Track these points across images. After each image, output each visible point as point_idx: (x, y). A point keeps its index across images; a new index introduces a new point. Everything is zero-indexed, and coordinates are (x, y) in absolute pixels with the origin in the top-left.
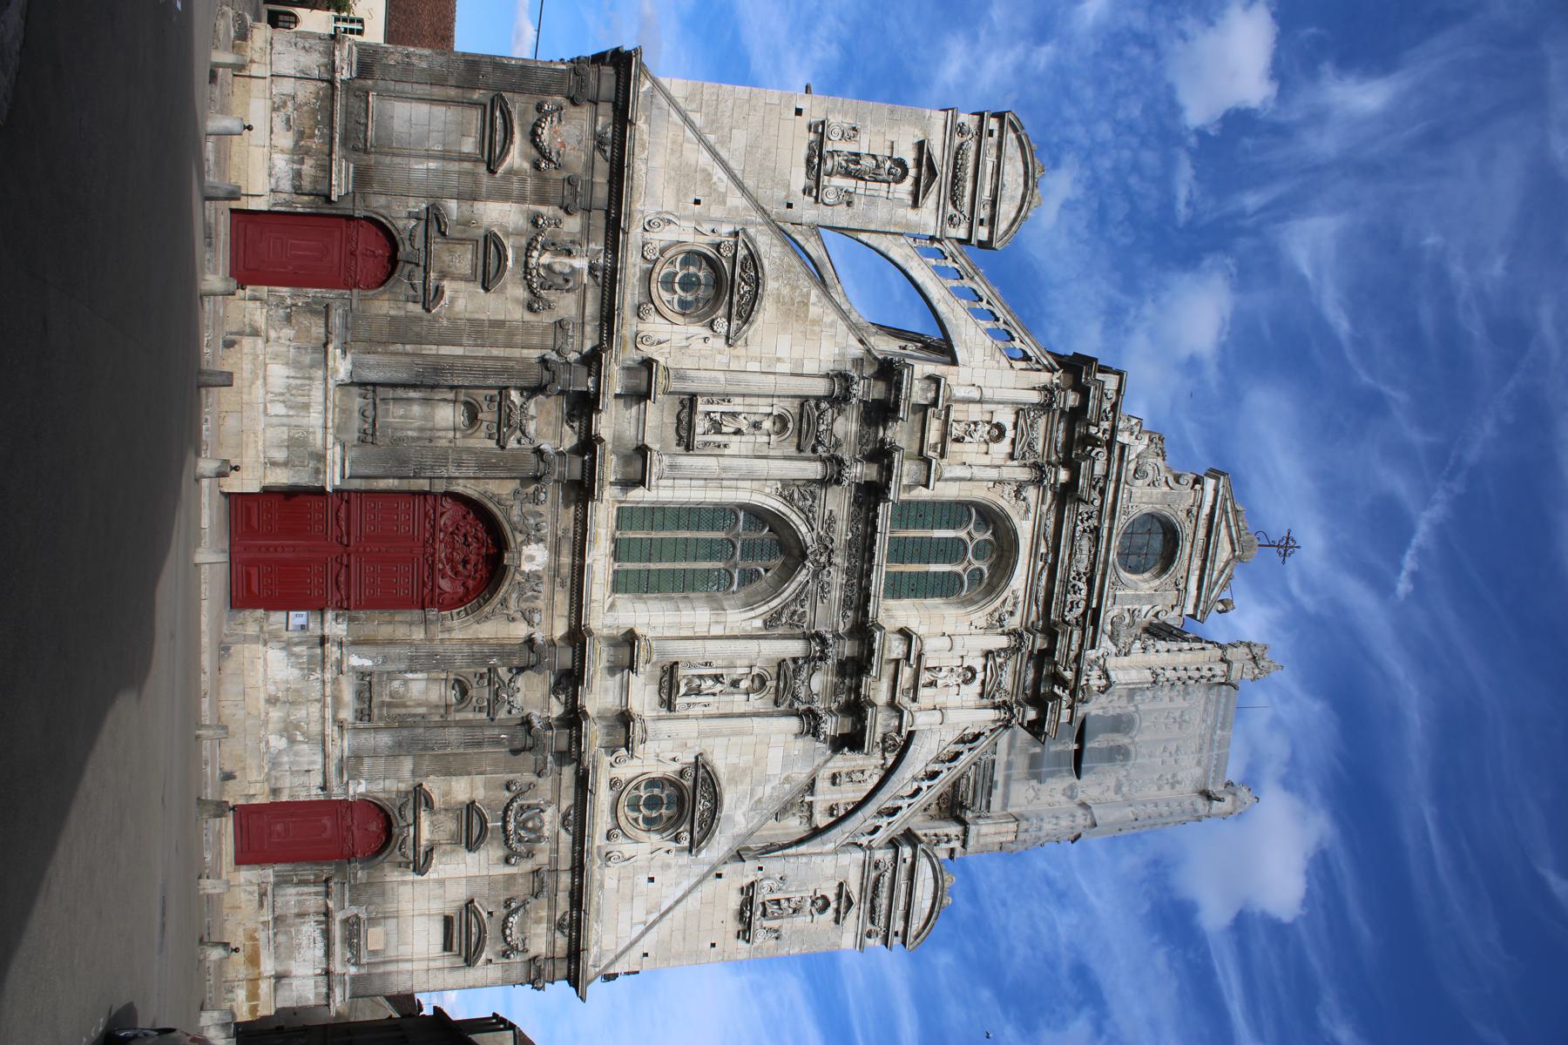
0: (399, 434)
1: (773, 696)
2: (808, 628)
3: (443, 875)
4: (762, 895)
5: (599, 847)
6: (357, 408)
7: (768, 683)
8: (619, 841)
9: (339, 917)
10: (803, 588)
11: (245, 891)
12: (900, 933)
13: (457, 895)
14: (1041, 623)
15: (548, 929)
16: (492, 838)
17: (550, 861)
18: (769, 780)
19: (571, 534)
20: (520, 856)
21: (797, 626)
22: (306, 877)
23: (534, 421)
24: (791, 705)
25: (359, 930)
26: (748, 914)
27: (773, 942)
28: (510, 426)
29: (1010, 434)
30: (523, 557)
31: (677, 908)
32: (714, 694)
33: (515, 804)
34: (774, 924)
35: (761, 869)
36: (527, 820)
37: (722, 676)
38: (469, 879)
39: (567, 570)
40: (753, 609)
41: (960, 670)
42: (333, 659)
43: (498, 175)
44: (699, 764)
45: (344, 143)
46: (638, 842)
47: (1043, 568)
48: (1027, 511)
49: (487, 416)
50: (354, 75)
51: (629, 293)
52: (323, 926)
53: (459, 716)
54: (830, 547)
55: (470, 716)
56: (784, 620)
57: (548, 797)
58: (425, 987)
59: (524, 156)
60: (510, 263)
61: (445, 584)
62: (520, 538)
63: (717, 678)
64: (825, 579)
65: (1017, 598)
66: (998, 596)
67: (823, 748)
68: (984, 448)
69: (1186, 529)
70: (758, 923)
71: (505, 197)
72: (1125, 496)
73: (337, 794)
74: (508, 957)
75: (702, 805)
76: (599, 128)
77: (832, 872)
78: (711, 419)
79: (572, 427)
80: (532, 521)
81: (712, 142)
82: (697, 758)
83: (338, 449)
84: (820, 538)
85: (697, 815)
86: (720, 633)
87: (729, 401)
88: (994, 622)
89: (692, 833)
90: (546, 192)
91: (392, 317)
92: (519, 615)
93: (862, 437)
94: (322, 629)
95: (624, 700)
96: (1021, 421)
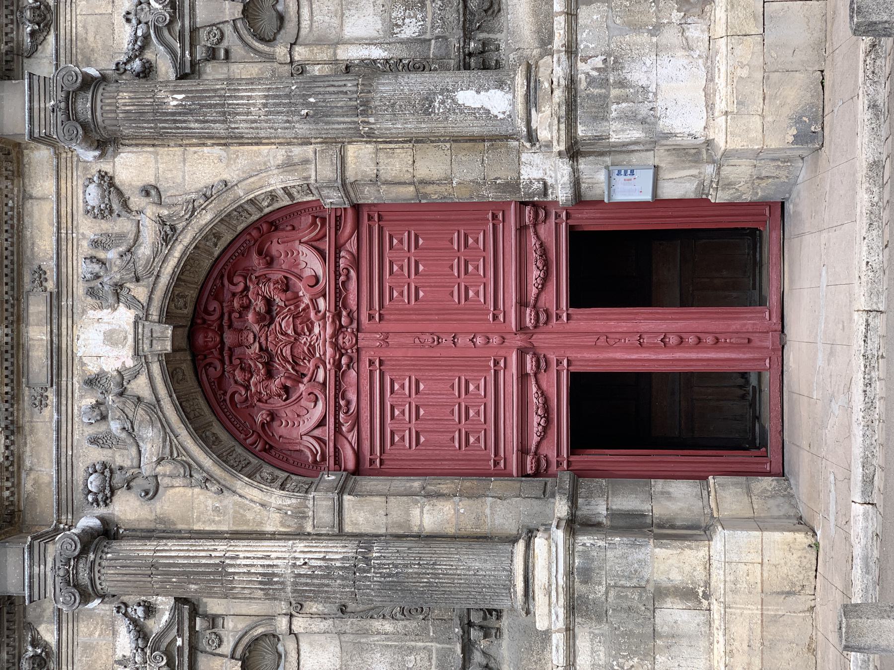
0: (412, 625)
23: (119, 655)
28: (167, 653)
30: (131, 338)
39: (32, 309)
42: (547, 110)
62: (140, 386)
79: (35, 643)
80: (115, 426)
92: (136, 201)
94: (575, 171)
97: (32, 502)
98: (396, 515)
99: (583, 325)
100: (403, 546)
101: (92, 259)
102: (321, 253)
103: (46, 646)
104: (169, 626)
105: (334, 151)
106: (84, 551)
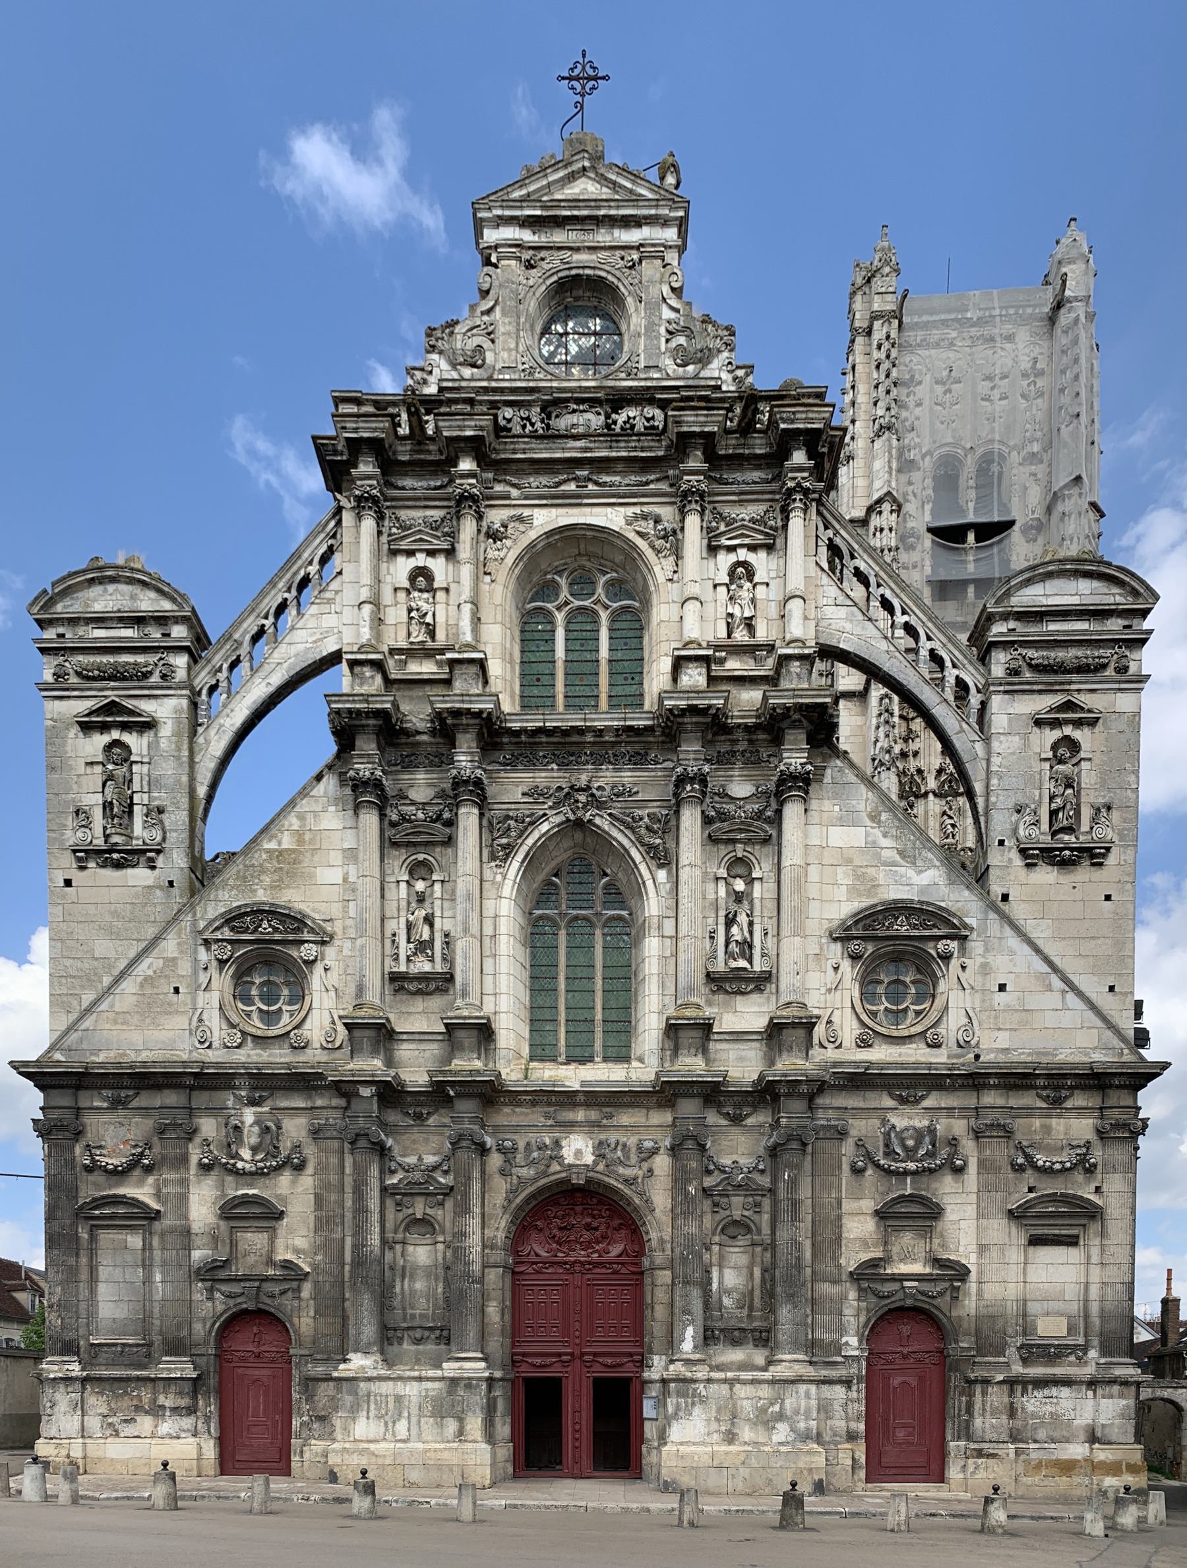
0: (441, 1302)
1: (757, 847)
2: (669, 808)
3: (974, 1248)
4: (1041, 835)
5: (949, 1057)
6: (413, 1347)
7: (740, 855)
8: (944, 1032)
9: (1018, 1369)
10: (618, 819)
11: (973, 1473)
12: (1126, 623)
13: (999, 1230)
14: (671, 472)
15: (1059, 1116)
16: (927, 1190)
17: (964, 1117)
18: (874, 842)
21: (667, 823)
22: (963, 1406)
23: (424, 1157)
24: (769, 821)
25: (1039, 1346)
26: (1067, 852)
27: (1115, 815)
29: (421, 560)
30: (578, 1162)
31: (1047, 950)
32: (751, 924)
33: (882, 1162)
34: (1086, 814)
35: (1001, 843)
37: (726, 916)
38: (980, 1216)
40: (644, 883)
41: (733, 587)
43: (162, 1210)
44: (843, 935)
45: (144, 1367)
46: (947, 1008)
47: (596, 483)
48: (520, 519)
49: (419, 1208)
50: (76, 1358)
51: (278, 1057)
52: (1030, 1387)
53: (766, 1230)
54: (566, 790)
56: (658, 841)
57: (877, 1122)
58: (1125, 1268)
59: (141, 1183)
60: (251, 1192)
62: (555, 1167)
63: (730, 921)
64: (608, 788)
65: (636, 517)
66: (635, 547)
67: (834, 770)
68: (440, 595)
69: (552, 261)
70: (1082, 838)
71: (183, 1200)
72: (507, 377)
73: (858, 1370)
74: (1095, 1166)
76: (105, 1105)
77: (1017, 738)
78: (415, 954)
79: (428, 1113)
80: (535, 1154)
81: (111, 979)
82: (835, 940)
84: (555, 806)
87: (394, 935)
88: (668, 545)
90: (176, 1158)
91: (316, 1312)
93: (432, 764)
95: (755, 1037)
96: (404, 545)
97: (498, 1112)
98: (493, 1294)
99: (584, 1384)
100: (479, 1299)
101: (618, 1143)
102: (620, 1256)
103: (427, 1119)
104: (440, 1183)
106: (475, 1144)
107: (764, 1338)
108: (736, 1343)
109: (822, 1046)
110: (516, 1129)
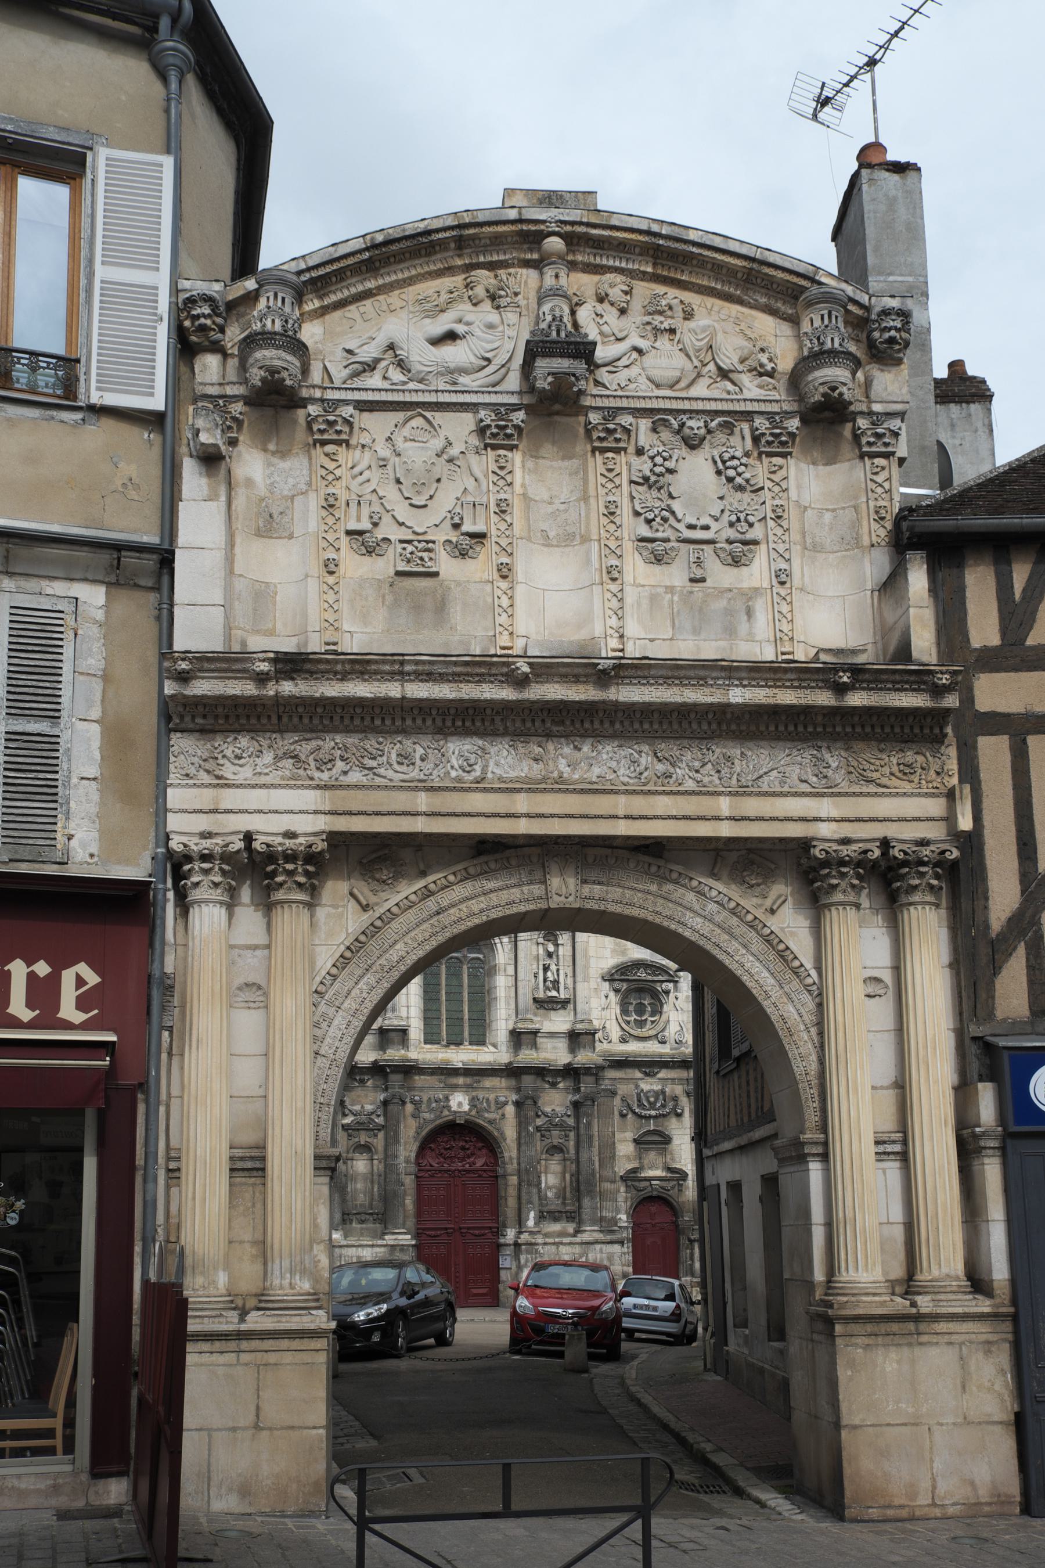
0: (376, 1197)
5: (671, 1049)
6: (359, 1226)
19: (443, 1077)
20: (675, 1106)
32: (558, 970)
36: (649, 1102)
44: (610, 978)
49: (363, 1138)
53: (572, 1151)
55: (572, 1143)
57: (632, 1086)
61: (480, 1163)
62: (446, 1112)
63: (546, 969)
75: (642, 975)
82: (605, 980)
83: (386, 1237)
85: (650, 978)
86: (513, 967)
89: (663, 981)
92: (500, 1112)
98: (409, 1192)
105: (515, 1172)
107: (574, 1216)
108: (556, 1220)
109: (600, 1041)
110: (422, 1089)
